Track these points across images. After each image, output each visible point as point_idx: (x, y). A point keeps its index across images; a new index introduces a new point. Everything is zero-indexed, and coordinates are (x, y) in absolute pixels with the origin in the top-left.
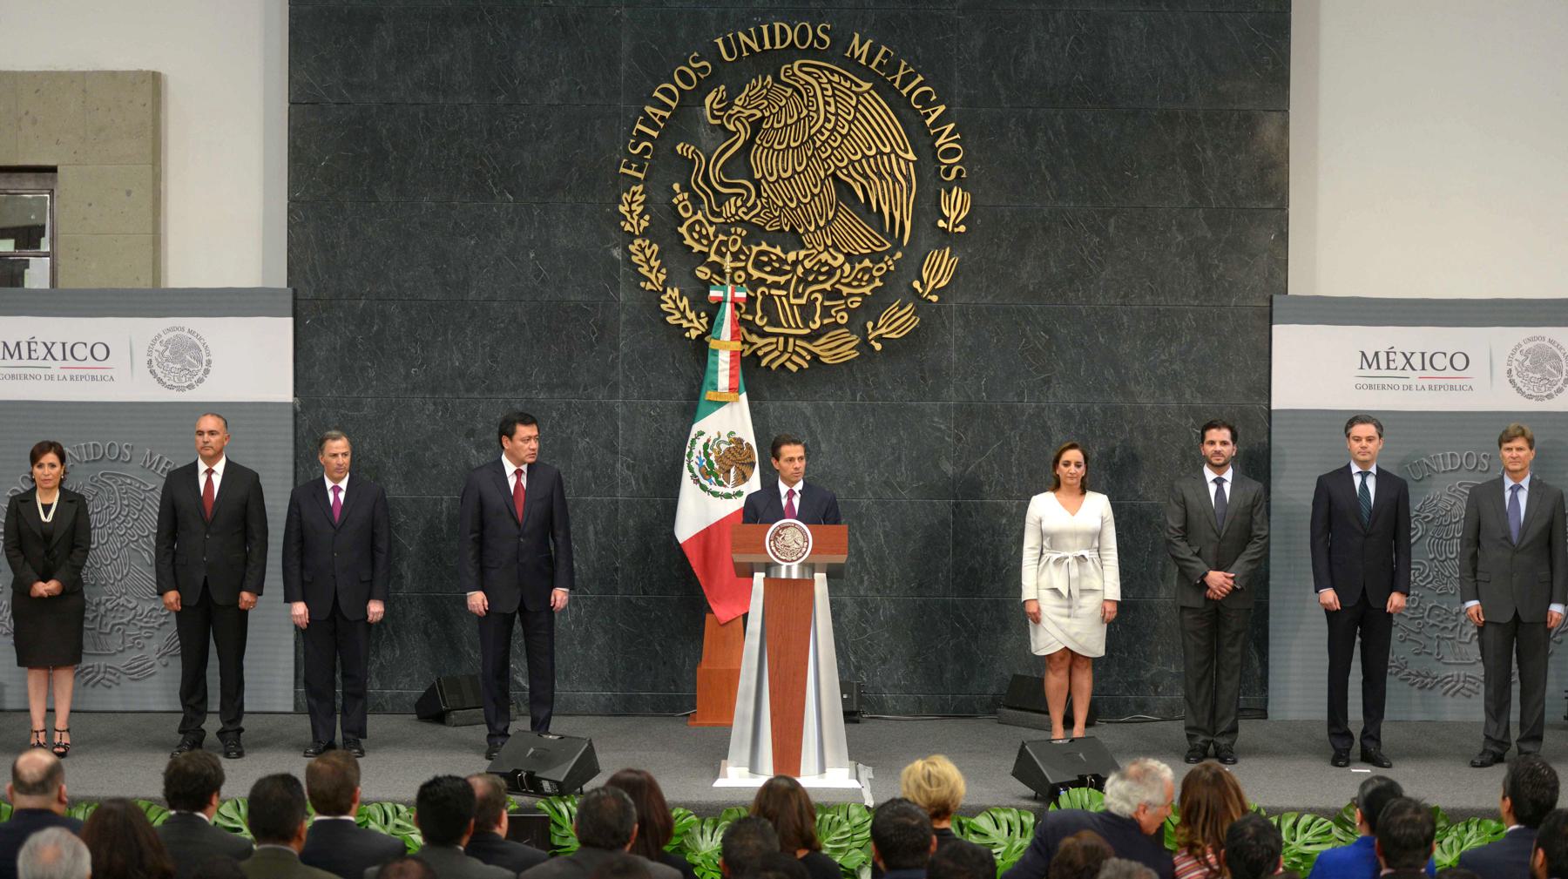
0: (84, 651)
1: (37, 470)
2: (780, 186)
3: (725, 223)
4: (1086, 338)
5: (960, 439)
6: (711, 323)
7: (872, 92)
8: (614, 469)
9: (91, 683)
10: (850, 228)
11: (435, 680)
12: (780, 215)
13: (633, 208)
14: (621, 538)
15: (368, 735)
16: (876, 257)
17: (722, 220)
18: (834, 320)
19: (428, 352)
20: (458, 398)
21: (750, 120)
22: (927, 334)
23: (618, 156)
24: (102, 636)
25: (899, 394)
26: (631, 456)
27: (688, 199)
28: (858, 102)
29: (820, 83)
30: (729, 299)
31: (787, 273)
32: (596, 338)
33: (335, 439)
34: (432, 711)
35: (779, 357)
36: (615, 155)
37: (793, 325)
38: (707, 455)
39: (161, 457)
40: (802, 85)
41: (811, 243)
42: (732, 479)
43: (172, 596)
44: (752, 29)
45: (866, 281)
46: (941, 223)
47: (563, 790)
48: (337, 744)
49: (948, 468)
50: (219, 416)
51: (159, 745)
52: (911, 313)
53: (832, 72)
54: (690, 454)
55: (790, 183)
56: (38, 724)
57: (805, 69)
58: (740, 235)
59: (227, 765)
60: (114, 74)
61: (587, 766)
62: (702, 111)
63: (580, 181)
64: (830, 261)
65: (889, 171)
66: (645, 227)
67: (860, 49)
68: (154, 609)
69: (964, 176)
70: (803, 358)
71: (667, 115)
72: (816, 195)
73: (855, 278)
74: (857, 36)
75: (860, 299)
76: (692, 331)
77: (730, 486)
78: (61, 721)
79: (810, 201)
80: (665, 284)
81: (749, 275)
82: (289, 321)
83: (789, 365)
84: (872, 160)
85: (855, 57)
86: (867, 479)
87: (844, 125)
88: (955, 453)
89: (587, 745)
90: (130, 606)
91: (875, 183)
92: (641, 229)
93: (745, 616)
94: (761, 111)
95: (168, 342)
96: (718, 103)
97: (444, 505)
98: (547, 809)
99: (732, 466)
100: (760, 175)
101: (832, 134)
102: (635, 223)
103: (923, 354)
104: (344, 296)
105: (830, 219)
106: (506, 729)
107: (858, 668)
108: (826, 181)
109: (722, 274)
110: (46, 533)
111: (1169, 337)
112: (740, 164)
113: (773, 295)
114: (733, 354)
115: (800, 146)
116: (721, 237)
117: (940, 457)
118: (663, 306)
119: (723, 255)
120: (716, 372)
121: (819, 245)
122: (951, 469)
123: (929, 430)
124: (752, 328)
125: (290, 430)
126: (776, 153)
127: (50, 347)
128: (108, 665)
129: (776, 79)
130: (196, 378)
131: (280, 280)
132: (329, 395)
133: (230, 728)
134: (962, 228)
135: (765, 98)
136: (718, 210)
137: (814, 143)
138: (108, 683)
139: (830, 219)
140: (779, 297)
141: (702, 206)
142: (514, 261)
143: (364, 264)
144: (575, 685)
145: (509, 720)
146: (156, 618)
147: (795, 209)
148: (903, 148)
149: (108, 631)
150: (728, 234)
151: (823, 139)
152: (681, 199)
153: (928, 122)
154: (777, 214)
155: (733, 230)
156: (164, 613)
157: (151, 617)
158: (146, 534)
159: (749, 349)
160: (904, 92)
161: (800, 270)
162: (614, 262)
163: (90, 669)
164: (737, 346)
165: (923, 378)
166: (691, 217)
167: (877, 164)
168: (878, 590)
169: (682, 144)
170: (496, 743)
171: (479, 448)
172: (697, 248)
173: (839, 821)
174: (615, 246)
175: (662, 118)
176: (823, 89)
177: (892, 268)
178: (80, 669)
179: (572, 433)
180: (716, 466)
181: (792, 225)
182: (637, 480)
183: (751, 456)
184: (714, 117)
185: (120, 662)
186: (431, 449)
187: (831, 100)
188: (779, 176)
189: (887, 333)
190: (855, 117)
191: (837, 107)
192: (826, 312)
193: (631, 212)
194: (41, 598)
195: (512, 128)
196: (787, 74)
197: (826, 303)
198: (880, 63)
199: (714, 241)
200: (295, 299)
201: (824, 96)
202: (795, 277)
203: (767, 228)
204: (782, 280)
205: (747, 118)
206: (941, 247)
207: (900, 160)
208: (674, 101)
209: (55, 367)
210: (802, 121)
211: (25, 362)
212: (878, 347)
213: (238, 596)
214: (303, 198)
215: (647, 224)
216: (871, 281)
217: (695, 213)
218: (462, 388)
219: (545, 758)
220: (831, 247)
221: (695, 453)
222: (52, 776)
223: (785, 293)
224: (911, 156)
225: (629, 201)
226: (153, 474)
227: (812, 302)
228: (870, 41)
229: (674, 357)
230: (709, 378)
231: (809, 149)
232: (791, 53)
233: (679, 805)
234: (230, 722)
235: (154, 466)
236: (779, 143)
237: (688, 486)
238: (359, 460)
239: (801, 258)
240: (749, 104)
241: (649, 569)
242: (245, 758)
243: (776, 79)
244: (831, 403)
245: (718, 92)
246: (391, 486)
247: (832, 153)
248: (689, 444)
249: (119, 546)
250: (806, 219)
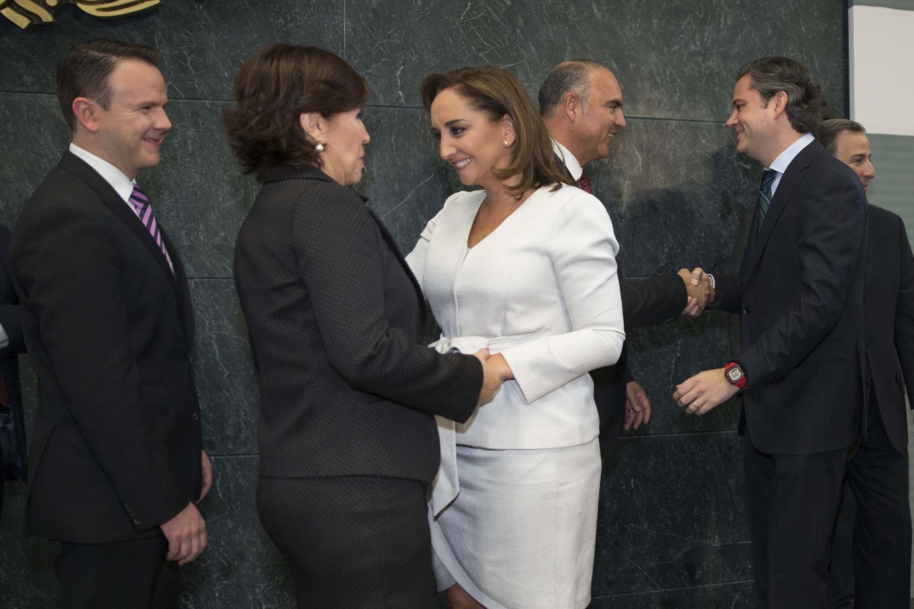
4: (572, 8)
111: (701, 16)
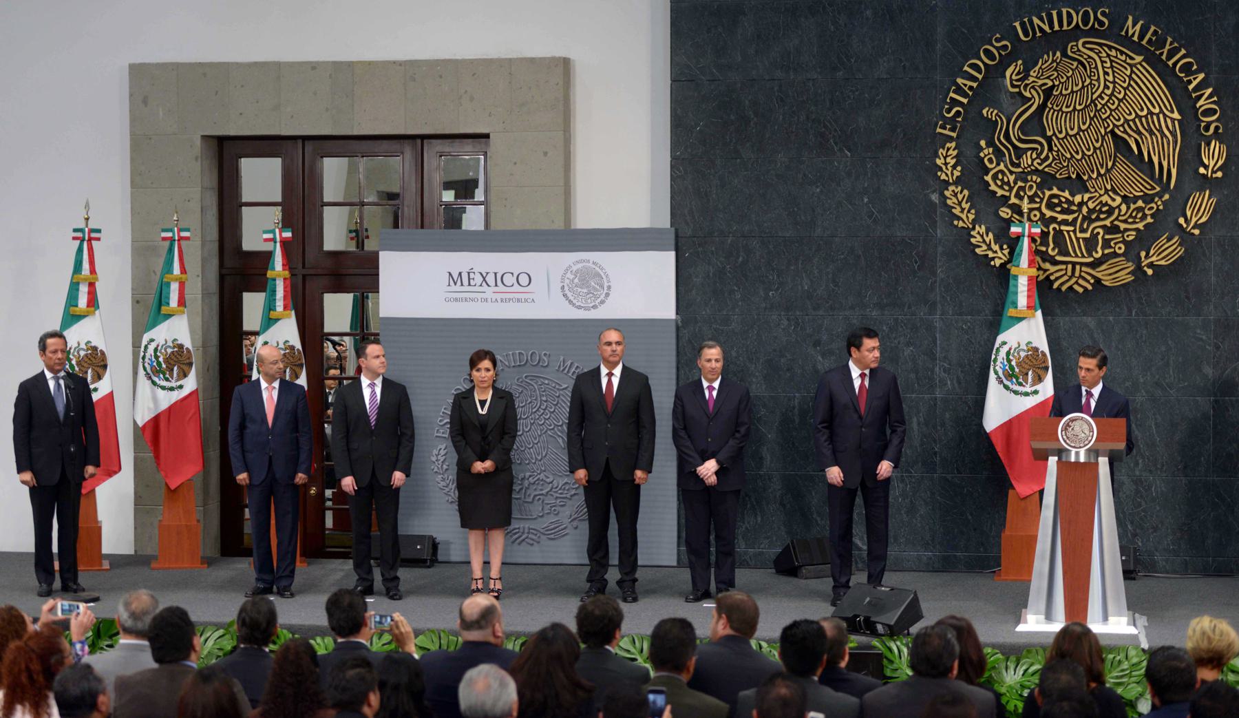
0: (513, 516)
1: (475, 373)
2: (1068, 141)
3: (1023, 172)
5: (1218, 348)
6: (1011, 253)
7: (1144, 64)
8: (933, 371)
9: (518, 541)
10: (1125, 175)
11: (789, 541)
12: (1068, 165)
13: (947, 161)
14: (939, 428)
15: (736, 584)
16: (1148, 199)
17: (1020, 170)
18: (1113, 250)
19: (783, 278)
20: (807, 315)
21: (1043, 88)
22: (1190, 261)
23: (935, 119)
24: (525, 505)
25: (1167, 310)
26: (947, 362)
27: (993, 153)
28: (1132, 72)
29: (1100, 57)
30: (1026, 234)
31: (1073, 212)
32: (919, 266)
33: (710, 347)
34: (787, 566)
35: (1067, 281)
36: (933, 118)
37: (1080, 255)
38: (1009, 361)
39: (572, 363)
40: (1086, 59)
41: (1094, 187)
42: (1030, 380)
43: (581, 473)
44: (1044, 14)
45: (1139, 218)
46: (1202, 170)
47: (894, 632)
48: (712, 592)
49: (1209, 371)
50: (619, 331)
51: (570, 591)
52: (1177, 244)
53: (1110, 48)
54: (995, 360)
55: (1076, 139)
56: (477, 573)
57: (1087, 46)
58: (1035, 182)
59: (625, 607)
60: (532, 61)
61: (913, 613)
62: (1003, 82)
63: (904, 140)
64: (1110, 202)
65: (1158, 128)
66: (957, 177)
67: (1133, 28)
68: (566, 483)
69: (1221, 131)
70: (1088, 281)
71: (975, 85)
72: (1097, 149)
73: (1130, 216)
74: (1131, 18)
75: (1134, 233)
76: (996, 260)
77: (1028, 386)
78: (494, 572)
79: (1093, 154)
80: (974, 222)
81: (1043, 215)
82: (673, 254)
83: (1076, 287)
84: (1143, 119)
85: (1130, 34)
86: (1142, 380)
87: (1120, 91)
88: (1214, 358)
89: (912, 596)
90: (548, 480)
91: (1146, 138)
92: (954, 178)
93: (1041, 492)
94: (1052, 80)
95: (577, 272)
96: (1016, 75)
97: (796, 401)
98: (880, 647)
99: (1029, 370)
100: (1051, 133)
101: (1110, 98)
102: (949, 173)
103: (1187, 277)
104: (716, 234)
105: (1109, 168)
106: (848, 581)
107: (1135, 535)
108: (1106, 137)
109: (1020, 213)
110: (483, 423)
112: (1035, 124)
113: (1062, 231)
114: (1030, 279)
115: (1084, 108)
116: (1020, 184)
117: (1202, 362)
118: (973, 240)
119: (1021, 198)
120: (1017, 293)
121: (1101, 189)
122: (1211, 372)
123: (1193, 340)
124: (1046, 257)
125: (674, 341)
126: (1064, 114)
127: (484, 276)
128: (531, 527)
129: (1064, 54)
130: (599, 300)
131: (665, 221)
132: (704, 313)
133: (626, 578)
134: (1219, 174)
135: (1055, 70)
136: (1017, 162)
137: (1096, 106)
138: (531, 542)
139: (1109, 168)
140: (1068, 232)
141: (1004, 159)
142: (851, 204)
143: (732, 207)
144: (903, 546)
145: (851, 574)
146: (568, 490)
147: (1081, 160)
148: (1169, 109)
149: (530, 500)
150: (1026, 181)
151: (1103, 102)
152: (987, 153)
153: (1191, 87)
154: (1065, 164)
155: (1029, 178)
156: (574, 487)
157: (564, 489)
158: (560, 423)
159: (1043, 274)
160: (1170, 63)
161: (1085, 210)
162: (932, 204)
163: (517, 530)
164: (1034, 272)
165: (1187, 298)
166: (994, 168)
167: (1148, 123)
168: (1151, 471)
169: (987, 109)
170: (839, 593)
171: (823, 355)
172: (1000, 192)
173: (1120, 660)
174: (933, 192)
175: (971, 88)
176: (1103, 62)
177: (1161, 207)
178: (508, 531)
179: (899, 343)
180: (1017, 370)
181: (1077, 172)
182: (952, 380)
183: (1045, 361)
184: (1013, 86)
185: (541, 525)
186: (786, 357)
187: (1110, 71)
188: (1067, 134)
189: (1157, 261)
190: (1129, 84)
191: (1114, 77)
192: (1107, 243)
193: (946, 164)
194: (479, 475)
195: (849, 97)
196: (1073, 50)
197: (1107, 237)
198: (1150, 40)
199: (1014, 187)
200: (677, 236)
201: (1103, 67)
202: (1081, 216)
203: (1058, 176)
204: (1070, 218)
205: (1040, 86)
206: (1202, 190)
207: (1167, 119)
208: (981, 74)
209: (489, 292)
210: (1086, 89)
211: (466, 288)
212: (1150, 272)
213: (633, 474)
214: (683, 157)
215: (959, 174)
216: (1144, 217)
217: (998, 164)
218: (810, 307)
219: (879, 606)
220: (1110, 190)
221: (1000, 359)
222: (487, 615)
223: (1072, 228)
224: (1176, 115)
225: (945, 155)
226: (565, 376)
227: (1094, 236)
228: (1141, 22)
229: (982, 282)
230: (1010, 298)
231: (1092, 111)
232: (1076, 33)
233: (988, 645)
234: (627, 574)
235: (567, 369)
236: (1067, 107)
237: (994, 389)
238: (728, 366)
239: (1085, 200)
240: (1042, 75)
241: (962, 453)
242: (639, 603)
243: (1064, 54)
244: (1111, 318)
245: (1016, 66)
246: (754, 386)
247: (1111, 114)
248: (994, 352)
249: (539, 434)
250: (1090, 169)
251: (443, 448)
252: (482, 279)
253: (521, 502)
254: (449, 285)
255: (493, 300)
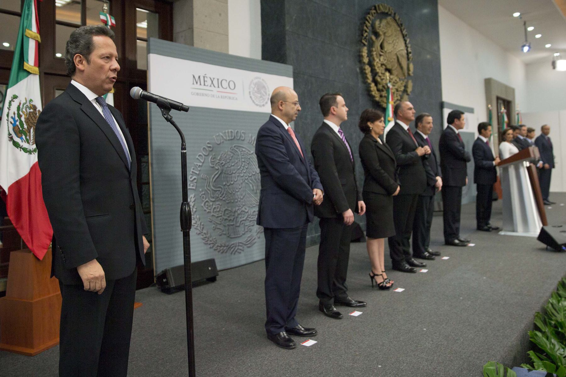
9: (234, 252)
24: (237, 228)
90: (246, 211)
112: (382, 47)
130: (265, 102)
185: (242, 240)
211: (202, 87)
251: (193, 196)
252: (211, 82)
253: (234, 226)
254: (193, 84)
255: (217, 96)
